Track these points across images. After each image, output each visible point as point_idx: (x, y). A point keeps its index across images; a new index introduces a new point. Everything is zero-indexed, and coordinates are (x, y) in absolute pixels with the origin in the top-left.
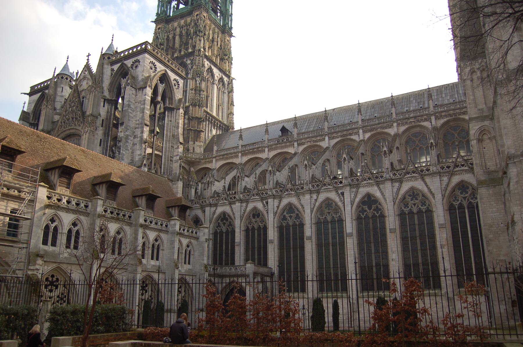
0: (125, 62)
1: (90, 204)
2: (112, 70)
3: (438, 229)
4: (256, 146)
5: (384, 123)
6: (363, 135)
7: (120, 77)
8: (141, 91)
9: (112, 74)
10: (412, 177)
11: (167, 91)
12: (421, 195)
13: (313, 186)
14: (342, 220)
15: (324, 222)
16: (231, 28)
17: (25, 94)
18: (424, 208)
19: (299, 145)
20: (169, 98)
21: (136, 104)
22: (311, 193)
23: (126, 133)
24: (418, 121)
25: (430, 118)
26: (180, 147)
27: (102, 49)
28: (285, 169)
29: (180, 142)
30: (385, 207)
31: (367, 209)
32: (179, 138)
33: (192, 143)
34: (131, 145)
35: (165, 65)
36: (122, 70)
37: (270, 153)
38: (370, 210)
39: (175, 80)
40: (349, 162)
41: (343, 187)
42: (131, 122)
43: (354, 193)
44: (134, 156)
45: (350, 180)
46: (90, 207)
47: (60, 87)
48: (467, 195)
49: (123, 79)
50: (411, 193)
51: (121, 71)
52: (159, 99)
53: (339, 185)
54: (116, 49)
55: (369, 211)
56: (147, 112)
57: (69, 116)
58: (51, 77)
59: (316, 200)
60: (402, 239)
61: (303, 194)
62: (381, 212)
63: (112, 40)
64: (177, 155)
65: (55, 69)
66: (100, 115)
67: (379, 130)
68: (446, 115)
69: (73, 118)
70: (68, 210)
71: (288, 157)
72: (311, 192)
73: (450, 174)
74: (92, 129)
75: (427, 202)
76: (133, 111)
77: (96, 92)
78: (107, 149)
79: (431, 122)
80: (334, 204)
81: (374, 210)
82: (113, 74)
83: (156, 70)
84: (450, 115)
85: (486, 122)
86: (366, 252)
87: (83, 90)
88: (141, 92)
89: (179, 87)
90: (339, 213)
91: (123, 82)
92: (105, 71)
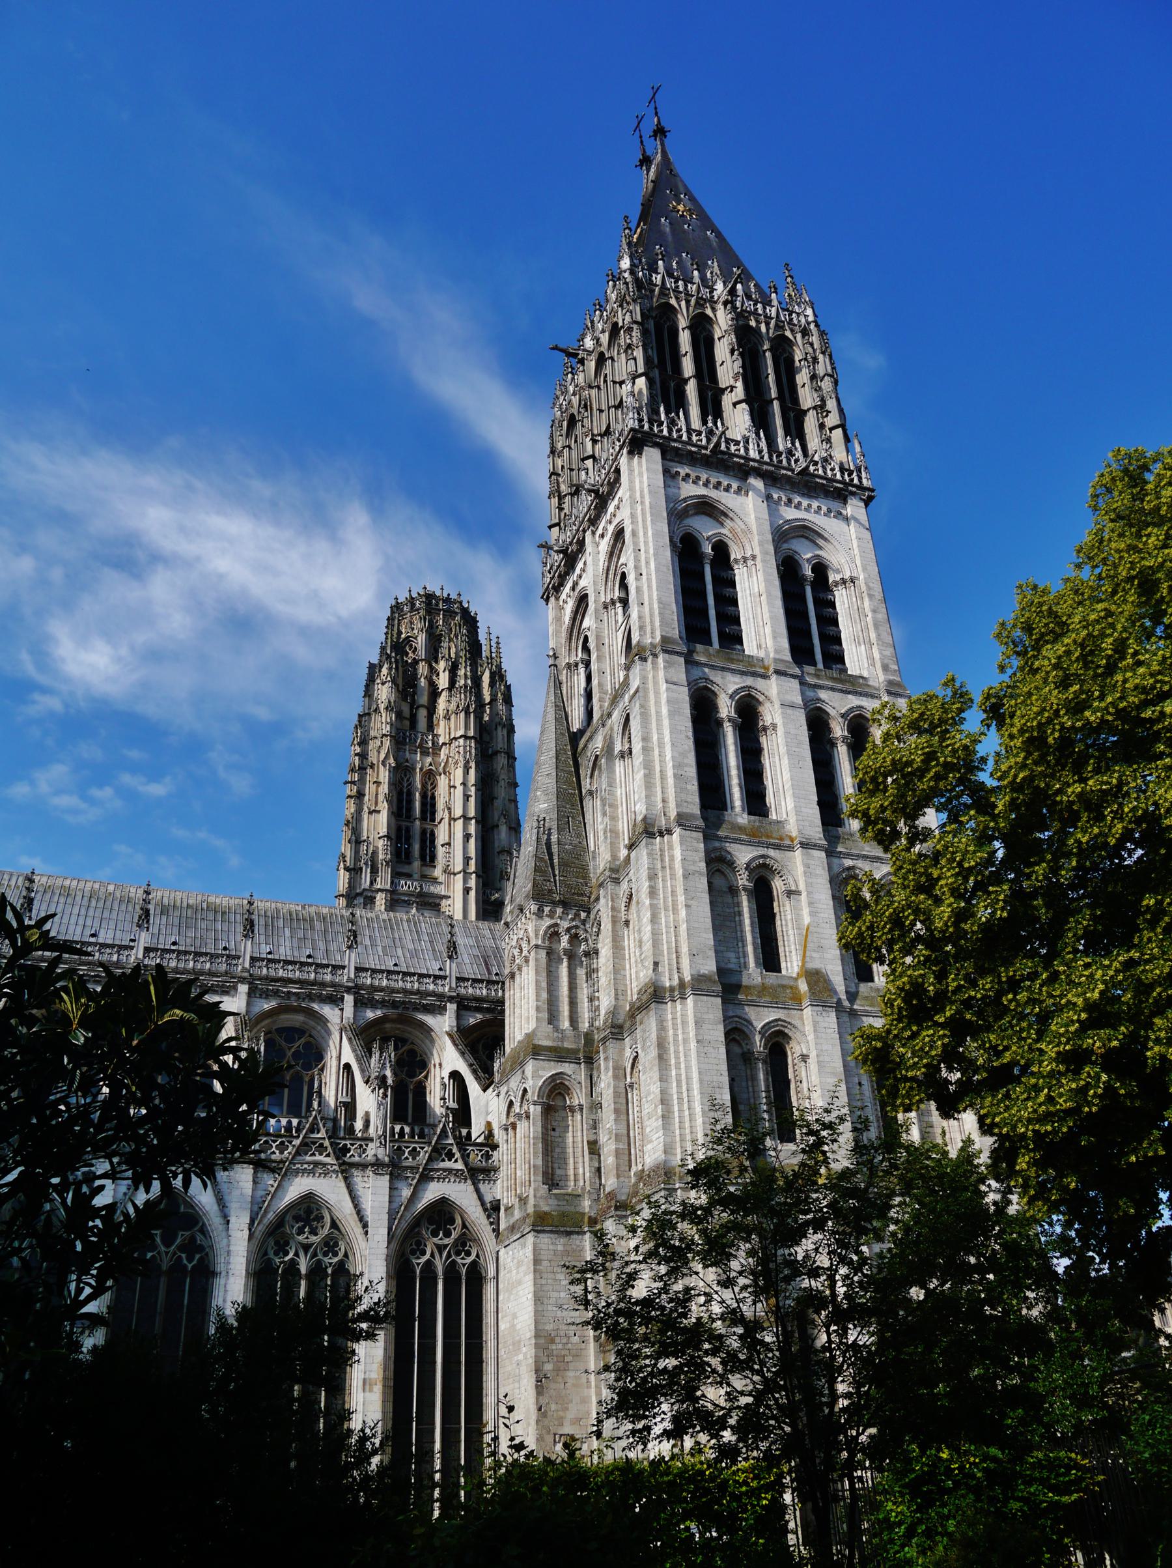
10: (316, 1164)
12: (327, 1219)
25: (342, 999)
30: (220, 1243)
38: (167, 1244)
48: (446, 1241)
50: (302, 1212)
55: (163, 1249)
62: (201, 1259)
79: (342, 1010)
81: (181, 1248)
84: (394, 1005)
85: (567, 1065)
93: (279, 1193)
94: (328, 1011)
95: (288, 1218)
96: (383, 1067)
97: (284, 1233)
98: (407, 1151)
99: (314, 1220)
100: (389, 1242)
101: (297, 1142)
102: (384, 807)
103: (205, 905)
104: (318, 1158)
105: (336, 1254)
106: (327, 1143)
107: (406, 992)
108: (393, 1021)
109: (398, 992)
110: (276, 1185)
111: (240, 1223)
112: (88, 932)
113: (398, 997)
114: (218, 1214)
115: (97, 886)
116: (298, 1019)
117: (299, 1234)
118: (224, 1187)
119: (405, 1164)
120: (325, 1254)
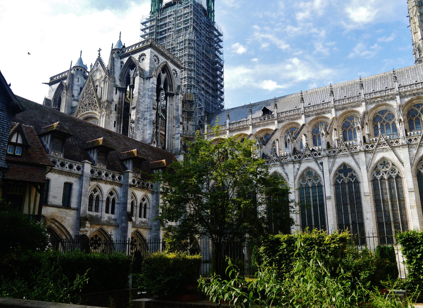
0: (133, 56)
1: (122, 176)
2: (122, 63)
3: (408, 192)
4: (241, 124)
5: (353, 102)
6: (336, 113)
7: (129, 68)
8: (148, 80)
9: (121, 66)
10: (383, 149)
11: (168, 79)
12: (391, 164)
13: (295, 158)
14: (322, 186)
15: (305, 187)
16: (214, 22)
17: (45, 83)
18: (394, 175)
19: (279, 122)
20: (170, 86)
21: (144, 91)
22: (294, 164)
23: (138, 116)
24: (385, 100)
25: (396, 98)
26: (180, 126)
27: (113, 44)
28: (269, 143)
29: (180, 122)
31: (343, 176)
32: (179, 119)
33: (186, 122)
34: (142, 126)
35: (166, 58)
36: (130, 62)
37: (254, 130)
38: (346, 177)
39: (174, 70)
40: (326, 137)
41: (321, 157)
42: (141, 106)
43: (331, 163)
44: (145, 135)
45: (328, 152)
46: (122, 179)
47: (77, 78)
49: (132, 70)
50: (382, 163)
51: (129, 63)
52: (162, 86)
53: (318, 156)
54: (123, 45)
55: (345, 178)
56: (154, 98)
57: (86, 102)
58: (69, 69)
59: (298, 169)
60: (375, 201)
61: (287, 164)
62: (356, 179)
63: (120, 37)
64: (178, 133)
65: (72, 62)
66: (113, 101)
67: (349, 109)
68: (410, 95)
69: (89, 104)
70: (106, 182)
71: (271, 133)
72: (294, 162)
73: (418, 146)
74: (107, 113)
75: (397, 170)
76: (143, 97)
77: (109, 82)
78: (120, 129)
79: (396, 101)
80: (314, 172)
81: (350, 177)
82: (123, 66)
83: (159, 62)
84: (414, 95)
86: (343, 213)
87: (96, 80)
88: (148, 81)
89: (177, 76)
90: (319, 180)
91: (132, 73)
92: (115, 63)
93: (374, 159)
94: (392, 103)
95: (378, 165)
96: (399, 116)
97: (377, 169)
98: (413, 139)
99: (386, 164)
100: (411, 167)
101: (376, 144)
102: (419, 30)
103: (354, 83)
104: (384, 147)
105: (395, 173)
106: (385, 142)
107: (417, 89)
108: (416, 99)
109: (415, 90)
110: (372, 157)
111: (364, 168)
112: (308, 104)
113: (415, 92)
114: (357, 167)
115: (324, 88)
116: (383, 108)
117: (382, 169)
118: (357, 160)
119: (413, 143)
120: (392, 173)
